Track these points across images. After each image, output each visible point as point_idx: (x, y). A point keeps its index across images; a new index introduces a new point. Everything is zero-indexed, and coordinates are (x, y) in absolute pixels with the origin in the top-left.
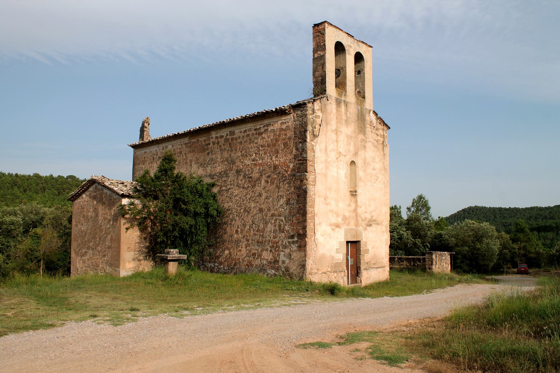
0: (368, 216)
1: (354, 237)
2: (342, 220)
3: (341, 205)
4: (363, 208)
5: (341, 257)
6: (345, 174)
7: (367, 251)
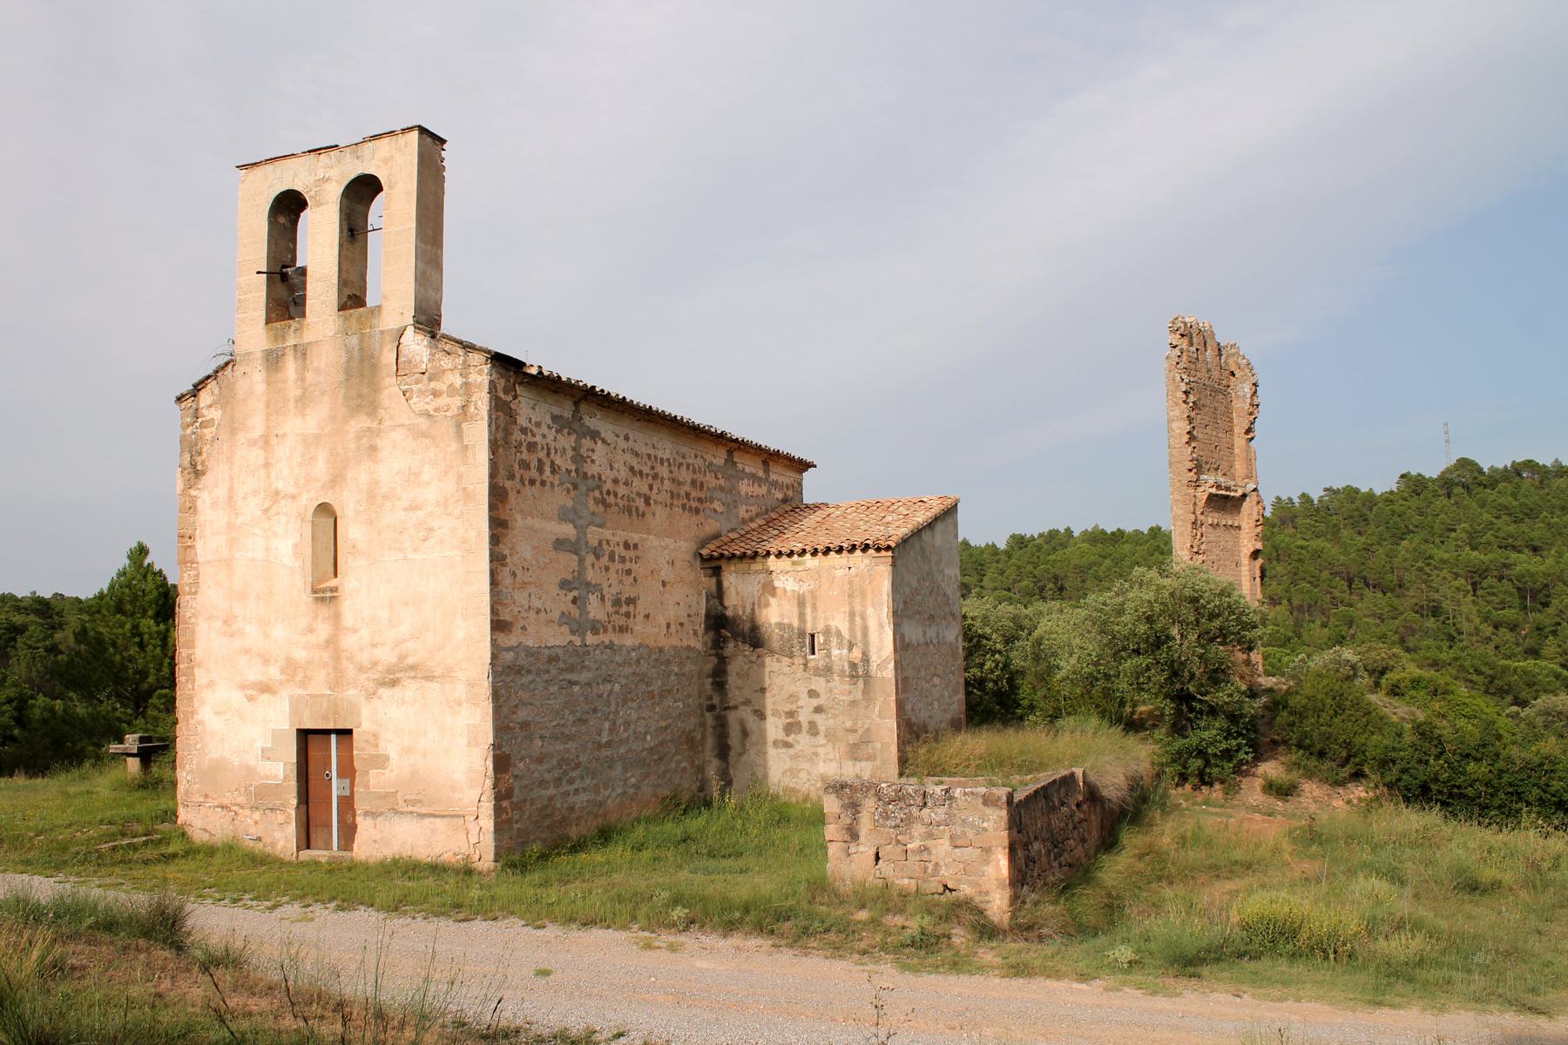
0: (386, 656)
1: (326, 718)
2: (283, 672)
3: (279, 632)
4: (365, 633)
5: (281, 769)
6: (295, 546)
7: (381, 761)
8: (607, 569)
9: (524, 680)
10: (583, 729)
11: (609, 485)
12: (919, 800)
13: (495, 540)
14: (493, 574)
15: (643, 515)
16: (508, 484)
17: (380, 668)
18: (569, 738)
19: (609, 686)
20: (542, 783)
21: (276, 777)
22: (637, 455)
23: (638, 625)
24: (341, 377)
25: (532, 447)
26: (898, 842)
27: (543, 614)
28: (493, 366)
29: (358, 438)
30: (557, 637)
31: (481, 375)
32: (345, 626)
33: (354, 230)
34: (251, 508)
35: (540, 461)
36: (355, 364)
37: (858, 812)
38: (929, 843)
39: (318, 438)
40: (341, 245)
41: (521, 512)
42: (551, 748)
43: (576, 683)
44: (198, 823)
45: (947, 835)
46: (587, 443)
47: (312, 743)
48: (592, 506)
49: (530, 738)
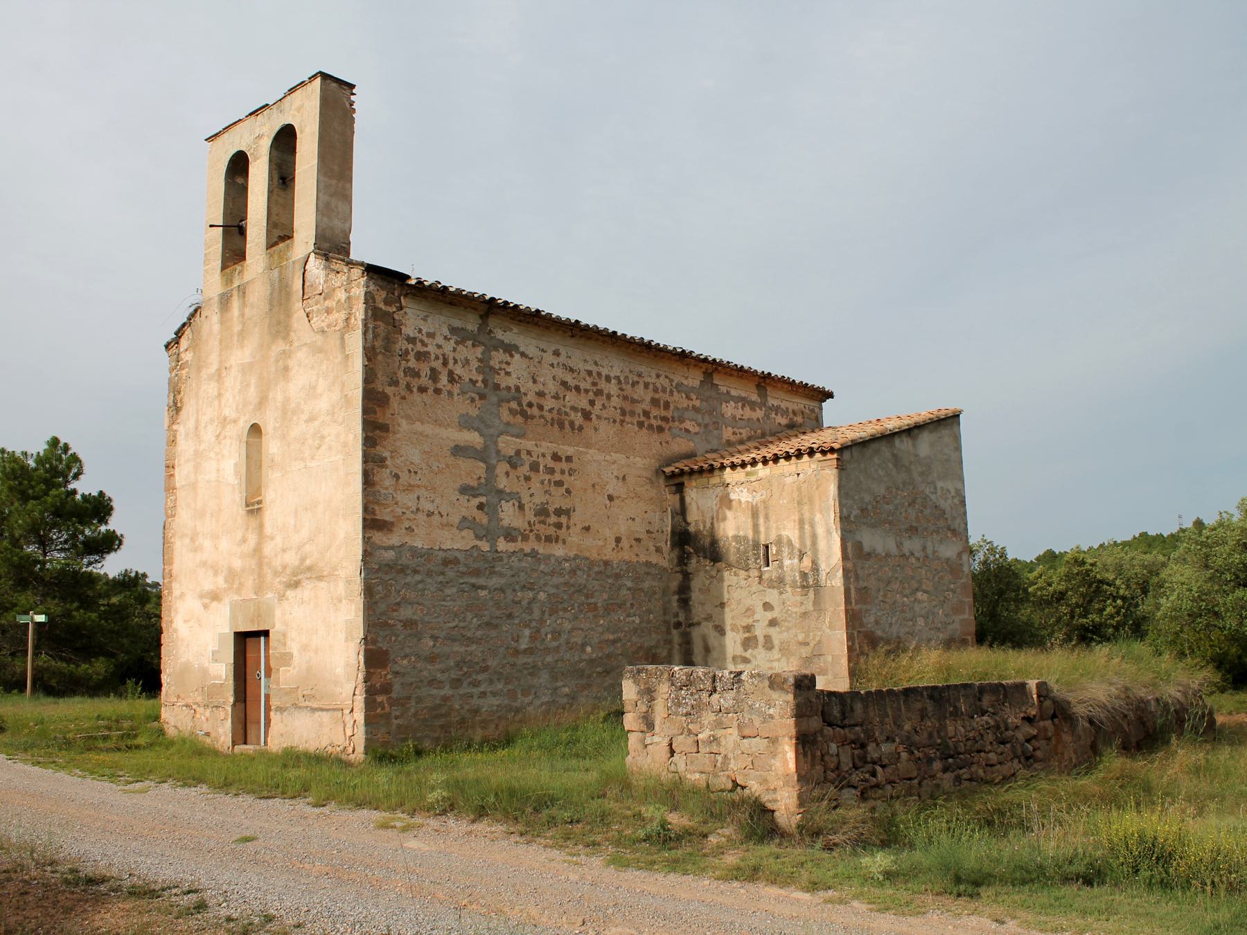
0: (291, 559)
1: (252, 621)
2: (226, 581)
3: (225, 544)
4: (278, 539)
5: (223, 670)
6: (236, 465)
7: (287, 658)
8: (527, 479)
9: (409, 579)
10: (493, 633)
11: (531, 397)
12: (708, 685)
13: (369, 442)
14: (366, 475)
15: (581, 428)
16: (389, 390)
17: (288, 571)
18: (471, 641)
19: (531, 594)
20: (432, 682)
21: (219, 677)
22: (572, 370)
23: (574, 537)
24: (268, 306)
25: (421, 356)
26: (690, 732)
27: (436, 517)
28: (370, 278)
29: (277, 361)
30: (459, 542)
31: (360, 287)
32: (258, 531)
33: (283, 178)
34: (209, 435)
35: (433, 370)
36: (276, 294)
37: (652, 699)
38: (719, 733)
39: (251, 365)
40: (270, 192)
41: (407, 417)
42: (446, 649)
43: (483, 588)
44: (172, 721)
45: (735, 724)
46: (498, 357)
47: (247, 642)
48: (505, 415)
49: (418, 636)
